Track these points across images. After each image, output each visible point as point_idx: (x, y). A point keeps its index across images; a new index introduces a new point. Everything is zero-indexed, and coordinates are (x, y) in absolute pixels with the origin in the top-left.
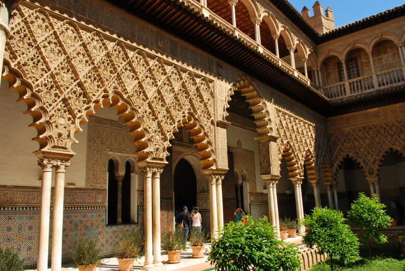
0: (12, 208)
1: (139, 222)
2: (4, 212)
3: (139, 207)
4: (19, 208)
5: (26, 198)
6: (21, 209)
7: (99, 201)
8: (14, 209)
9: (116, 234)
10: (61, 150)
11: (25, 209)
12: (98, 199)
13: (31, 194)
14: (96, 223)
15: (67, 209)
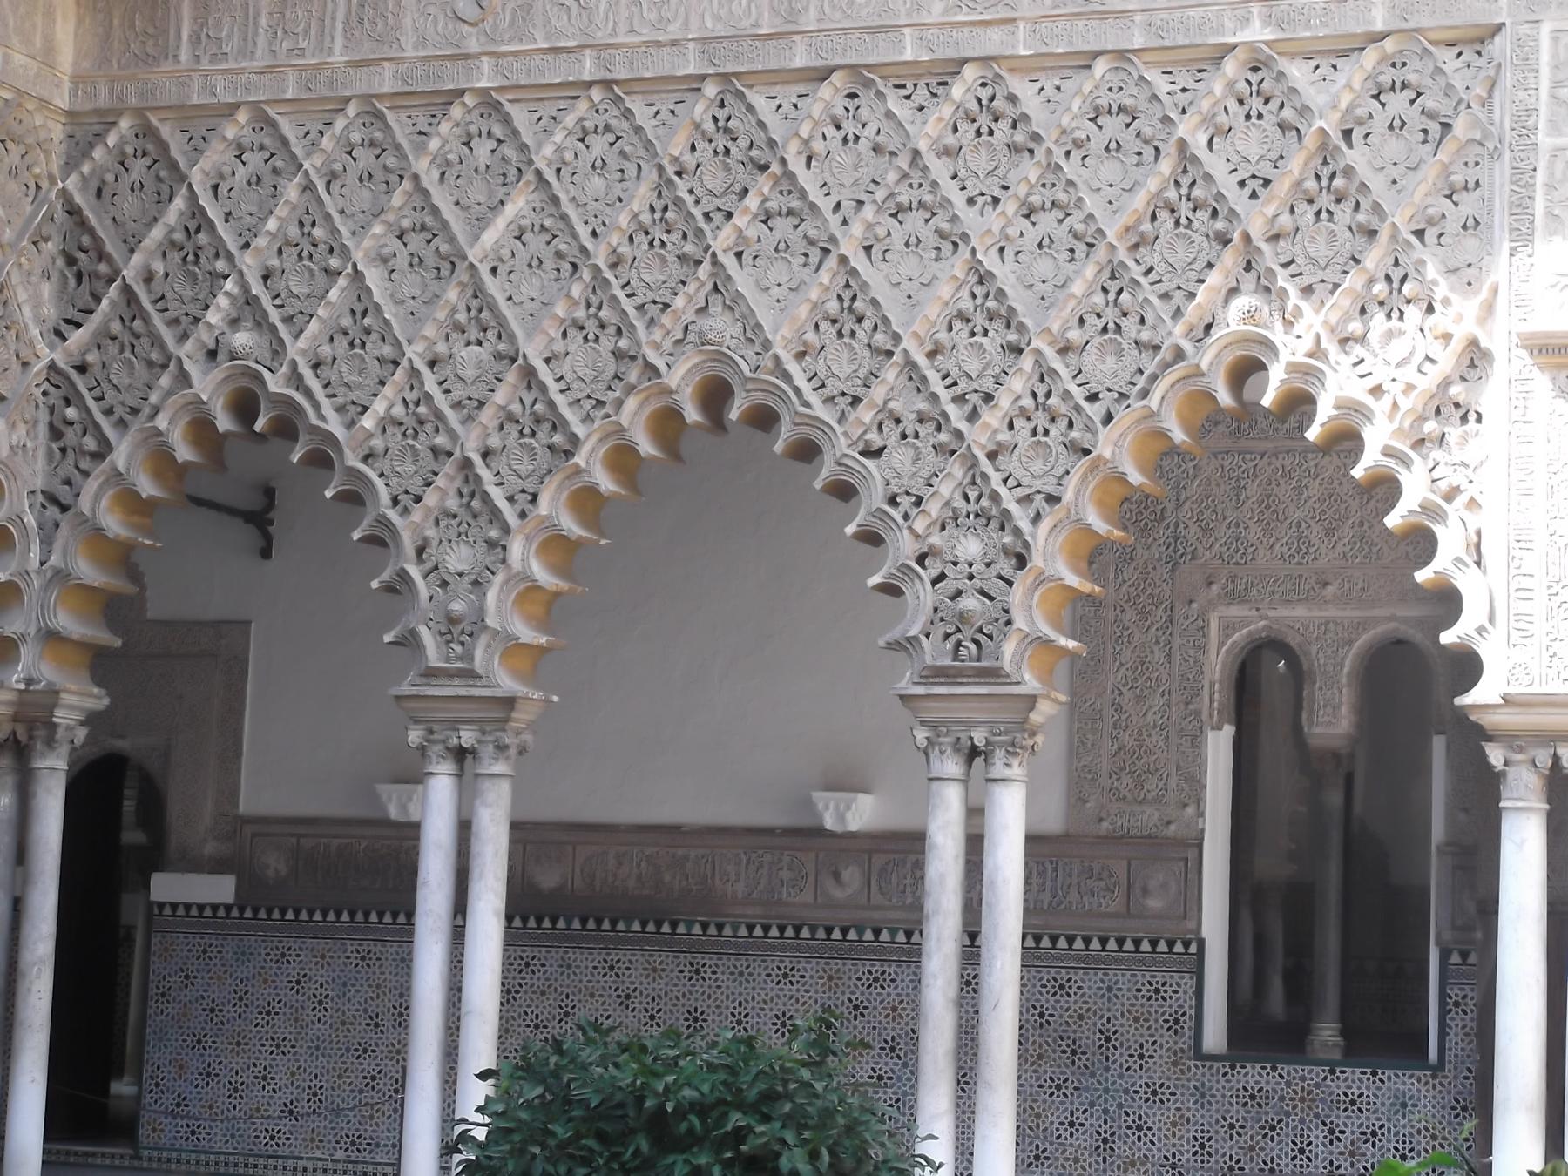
0: (705, 926)
1: (1450, 1056)
2: (1121, 961)
3: (1455, 958)
4: (735, 928)
5: (764, 881)
6: (743, 932)
7: (1154, 903)
8: (712, 930)
9: (1271, 1115)
10: (457, 682)
11: (758, 932)
12: (1145, 892)
13: (786, 859)
14: (1129, 1034)
15: (1046, 942)
